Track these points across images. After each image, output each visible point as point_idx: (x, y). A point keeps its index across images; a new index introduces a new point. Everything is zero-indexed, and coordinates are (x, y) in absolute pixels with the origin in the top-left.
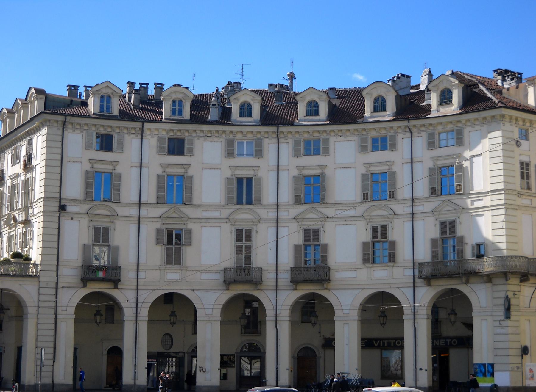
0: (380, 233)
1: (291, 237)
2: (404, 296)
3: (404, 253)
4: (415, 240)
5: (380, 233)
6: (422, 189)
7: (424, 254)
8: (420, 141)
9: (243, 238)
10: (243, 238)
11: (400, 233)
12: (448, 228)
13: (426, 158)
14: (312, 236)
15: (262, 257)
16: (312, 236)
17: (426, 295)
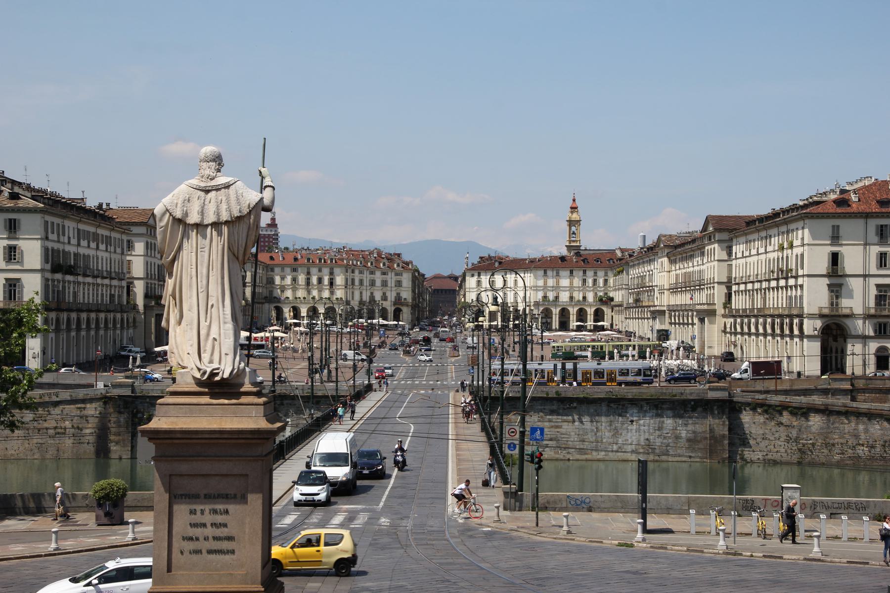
0: (384, 294)
1: (369, 294)
2: (389, 308)
3: (389, 299)
4: (391, 296)
5: (384, 294)
6: (393, 285)
7: (393, 300)
8: (393, 274)
9: (361, 293)
10: (361, 293)
11: (388, 294)
12: (398, 294)
13: (395, 278)
14: (372, 293)
15: (364, 299)
16: (372, 293)
17: (393, 308)
